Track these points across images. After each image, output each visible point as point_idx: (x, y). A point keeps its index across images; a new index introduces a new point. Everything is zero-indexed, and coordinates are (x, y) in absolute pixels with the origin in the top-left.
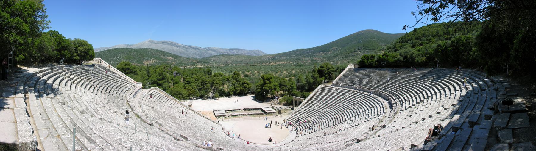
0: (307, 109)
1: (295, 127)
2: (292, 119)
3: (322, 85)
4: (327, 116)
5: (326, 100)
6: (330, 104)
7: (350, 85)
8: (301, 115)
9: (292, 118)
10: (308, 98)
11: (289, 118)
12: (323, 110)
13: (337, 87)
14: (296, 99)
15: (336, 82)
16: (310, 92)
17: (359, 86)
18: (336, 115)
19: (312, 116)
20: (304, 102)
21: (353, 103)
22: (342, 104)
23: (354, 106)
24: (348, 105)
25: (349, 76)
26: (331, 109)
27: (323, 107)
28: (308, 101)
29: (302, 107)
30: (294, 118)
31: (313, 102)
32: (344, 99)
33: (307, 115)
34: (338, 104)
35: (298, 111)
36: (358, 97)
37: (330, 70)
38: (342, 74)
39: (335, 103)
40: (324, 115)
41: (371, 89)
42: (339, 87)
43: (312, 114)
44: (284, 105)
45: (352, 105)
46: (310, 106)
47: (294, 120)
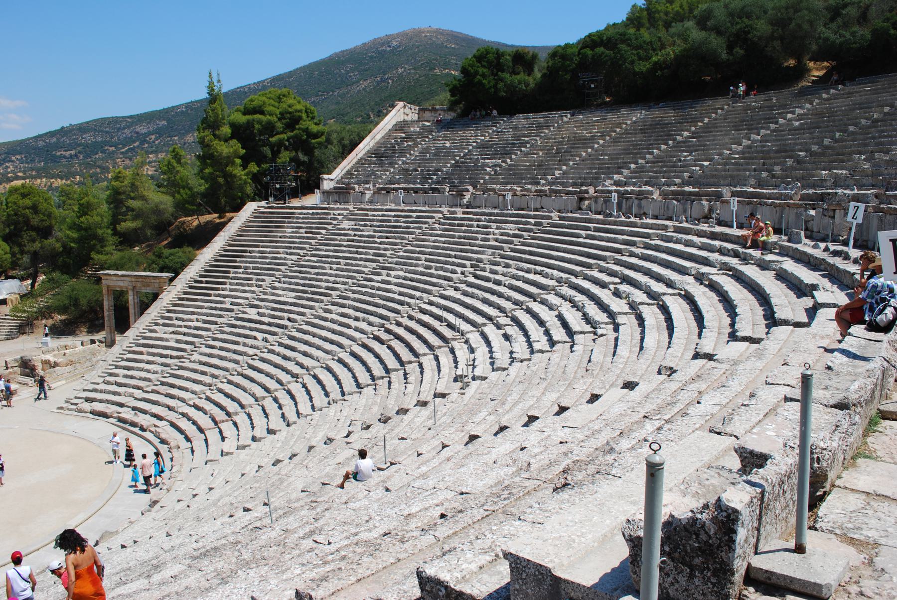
1: (143, 429)
2: (114, 388)
3: (263, 203)
4: (326, 339)
5: (302, 266)
6: (327, 281)
8: (168, 361)
10: (191, 272)
12: (292, 316)
14: (121, 284)
16: (198, 249)
19: (235, 352)
25: (403, 152)
26: (343, 306)
28: (191, 287)
29: (163, 318)
30: (125, 385)
31: (228, 286)
35: (146, 343)
37: (299, 129)
38: (368, 148)
44: (58, 331)
45: (464, 266)
46: (216, 309)
47: (132, 396)
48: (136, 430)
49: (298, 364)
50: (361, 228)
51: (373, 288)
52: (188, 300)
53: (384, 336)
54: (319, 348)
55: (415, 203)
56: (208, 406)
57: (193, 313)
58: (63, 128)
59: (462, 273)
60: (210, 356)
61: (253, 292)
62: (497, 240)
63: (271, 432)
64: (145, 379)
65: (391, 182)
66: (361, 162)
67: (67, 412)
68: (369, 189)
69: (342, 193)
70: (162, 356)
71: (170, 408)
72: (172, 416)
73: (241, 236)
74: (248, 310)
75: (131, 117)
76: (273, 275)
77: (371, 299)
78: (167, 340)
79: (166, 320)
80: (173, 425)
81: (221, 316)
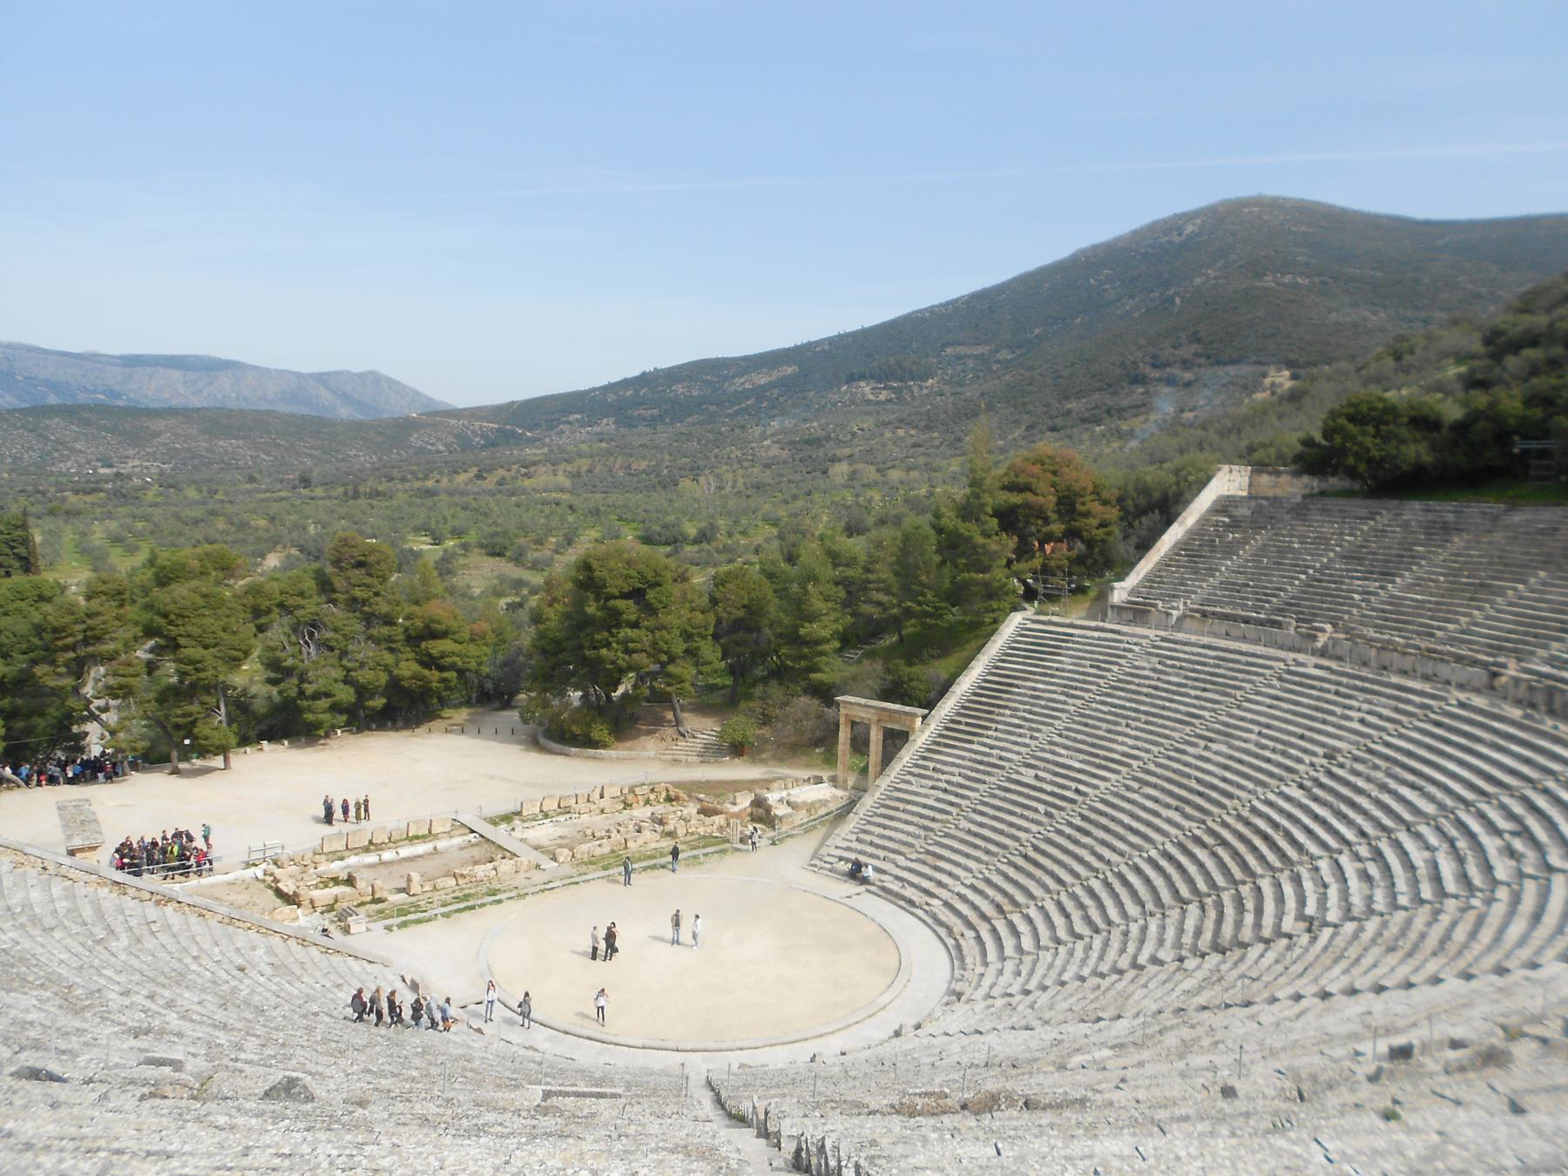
0: (961, 780)
5: (1089, 717)
7: (1261, 623)
8: (931, 824)
9: (871, 844)
10: (947, 706)
11: (848, 849)
12: (1082, 788)
13: (1151, 633)
14: (862, 714)
15: (1133, 592)
17: (1334, 625)
18: (1204, 822)
19: (1012, 825)
20: (924, 733)
21: (1323, 745)
22: (1223, 748)
23: (1341, 766)
27: (1077, 765)
28: (947, 729)
33: (979, 818)
34: (1195, 745)
36: (1350, 708)
39: (1167, 737)
40: (1103, 821)
42: (1163, 634)
43: (1011, 813)
45: (1314, 754)
46: (981, 763)
49: (1094, 853)
50: (1168, 670)
51: (1186, 764)
52: (947, 746)
53: (1209, 840)
54: (1122, 839)
56: (990, 892)
57: (953, 765)
58: (644, 374)
59: (1312, 765)
60: (981, 825)
61: (1027, 746)
62: (1362, 721)
63: (1155, 960)
65: (1209, 602)
66: (1165, 564)
68: (1177, 608)
69: (1137, 612)
70: (922, 816)
71: (940, 884)
72: (945, 894)
73: (1003, 661)
74: (1023, 770)
75: (745, 359)
79: (919, 770)
80: (946, 904)
81: (989, 774)
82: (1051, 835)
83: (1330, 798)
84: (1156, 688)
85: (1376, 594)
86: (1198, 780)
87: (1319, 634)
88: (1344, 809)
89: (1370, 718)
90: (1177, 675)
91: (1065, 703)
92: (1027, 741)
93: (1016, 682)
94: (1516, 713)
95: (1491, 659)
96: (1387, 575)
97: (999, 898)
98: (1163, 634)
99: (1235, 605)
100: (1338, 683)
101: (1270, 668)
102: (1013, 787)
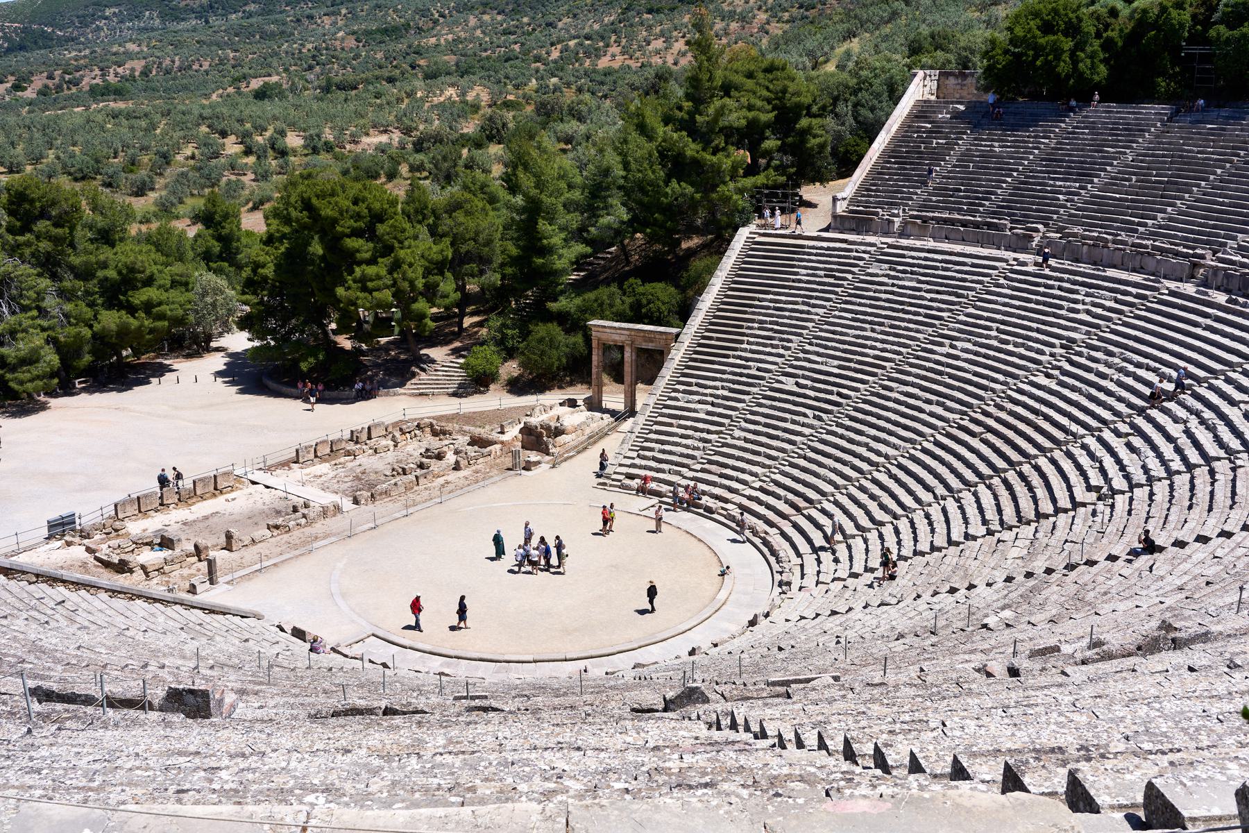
0: (726, 393)
1: (709, 510)
2: (653, 464)
7: (977, 225)
8: (704, 435)
9: (654, 459)
11: (633, 466)
17: (1046, 225)
22: (969, 346)
23: (1080, 354)
24: (1022, 351)
32: (968, 315)
34: (941, 345)
35: (667, 411)
36: (1076, 301)
38: (883, 147)
40: (869, 418)
41: (1154, 248)
42: (889, 240)
45: (1052, 345)
46: (741, 375)
48: (701, 511)
49: (870, 449)
50: (900, 275)
55: (963, 240)
59: (1052, 355)
61: (781, 356)
62: (1088, 312)
64: (688, 456)
65: (924, 207)
67: (612, 489)
68: (897, 216)
72: (738, 499)
74: (783, 379)
76: (800, 335)
77: (938, 377)
78: (695, 411)
82: (824, 436)
83: (1077, 384)
84: (892, 293)
85: (1078, 194)
86: (951, 376)
87: (1034, 234)
88: (1093, 392)
89: (1094, 309)
90: (911, 280)
91: (808, 313)
92: (781, 351)
93: (757, 295)
94: (1221, 298)
95: (1191, 252)
96: (1085, 175)
97: (790, 496)
98: (889, 240)
99: (951, 210)
100: (1061, 280)
101: (995, 268)
102: (777, 395)
